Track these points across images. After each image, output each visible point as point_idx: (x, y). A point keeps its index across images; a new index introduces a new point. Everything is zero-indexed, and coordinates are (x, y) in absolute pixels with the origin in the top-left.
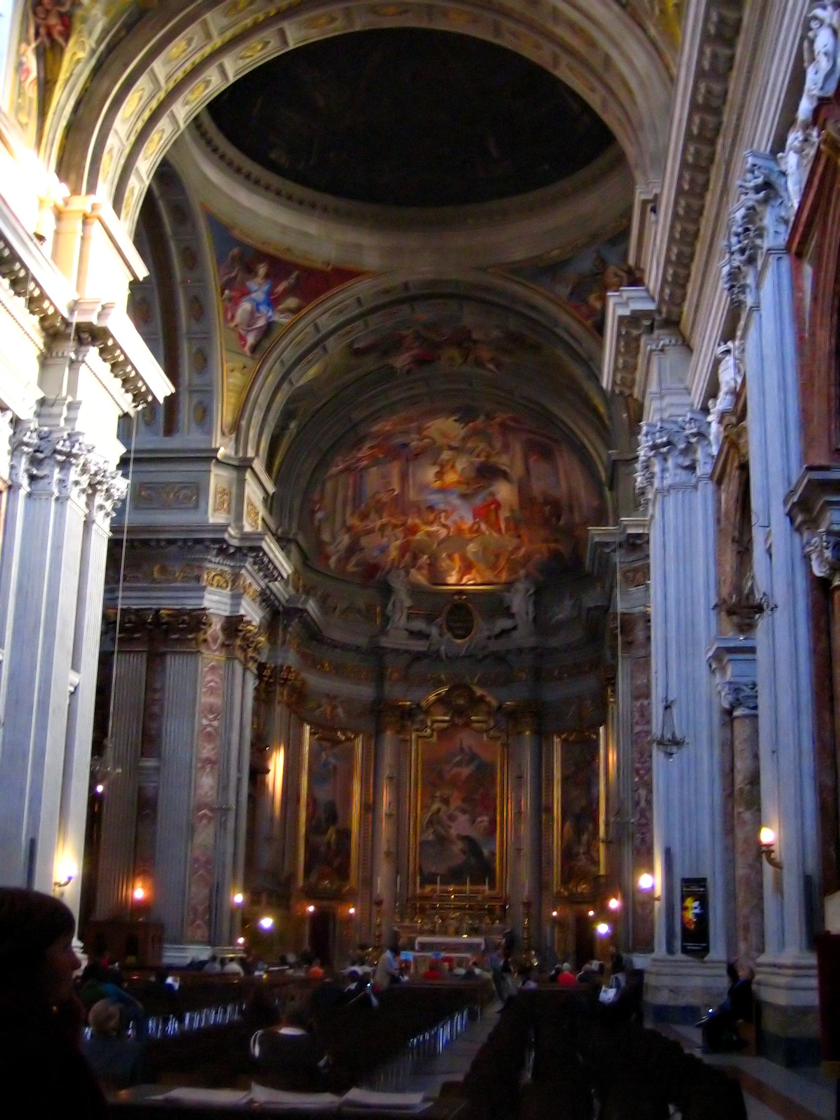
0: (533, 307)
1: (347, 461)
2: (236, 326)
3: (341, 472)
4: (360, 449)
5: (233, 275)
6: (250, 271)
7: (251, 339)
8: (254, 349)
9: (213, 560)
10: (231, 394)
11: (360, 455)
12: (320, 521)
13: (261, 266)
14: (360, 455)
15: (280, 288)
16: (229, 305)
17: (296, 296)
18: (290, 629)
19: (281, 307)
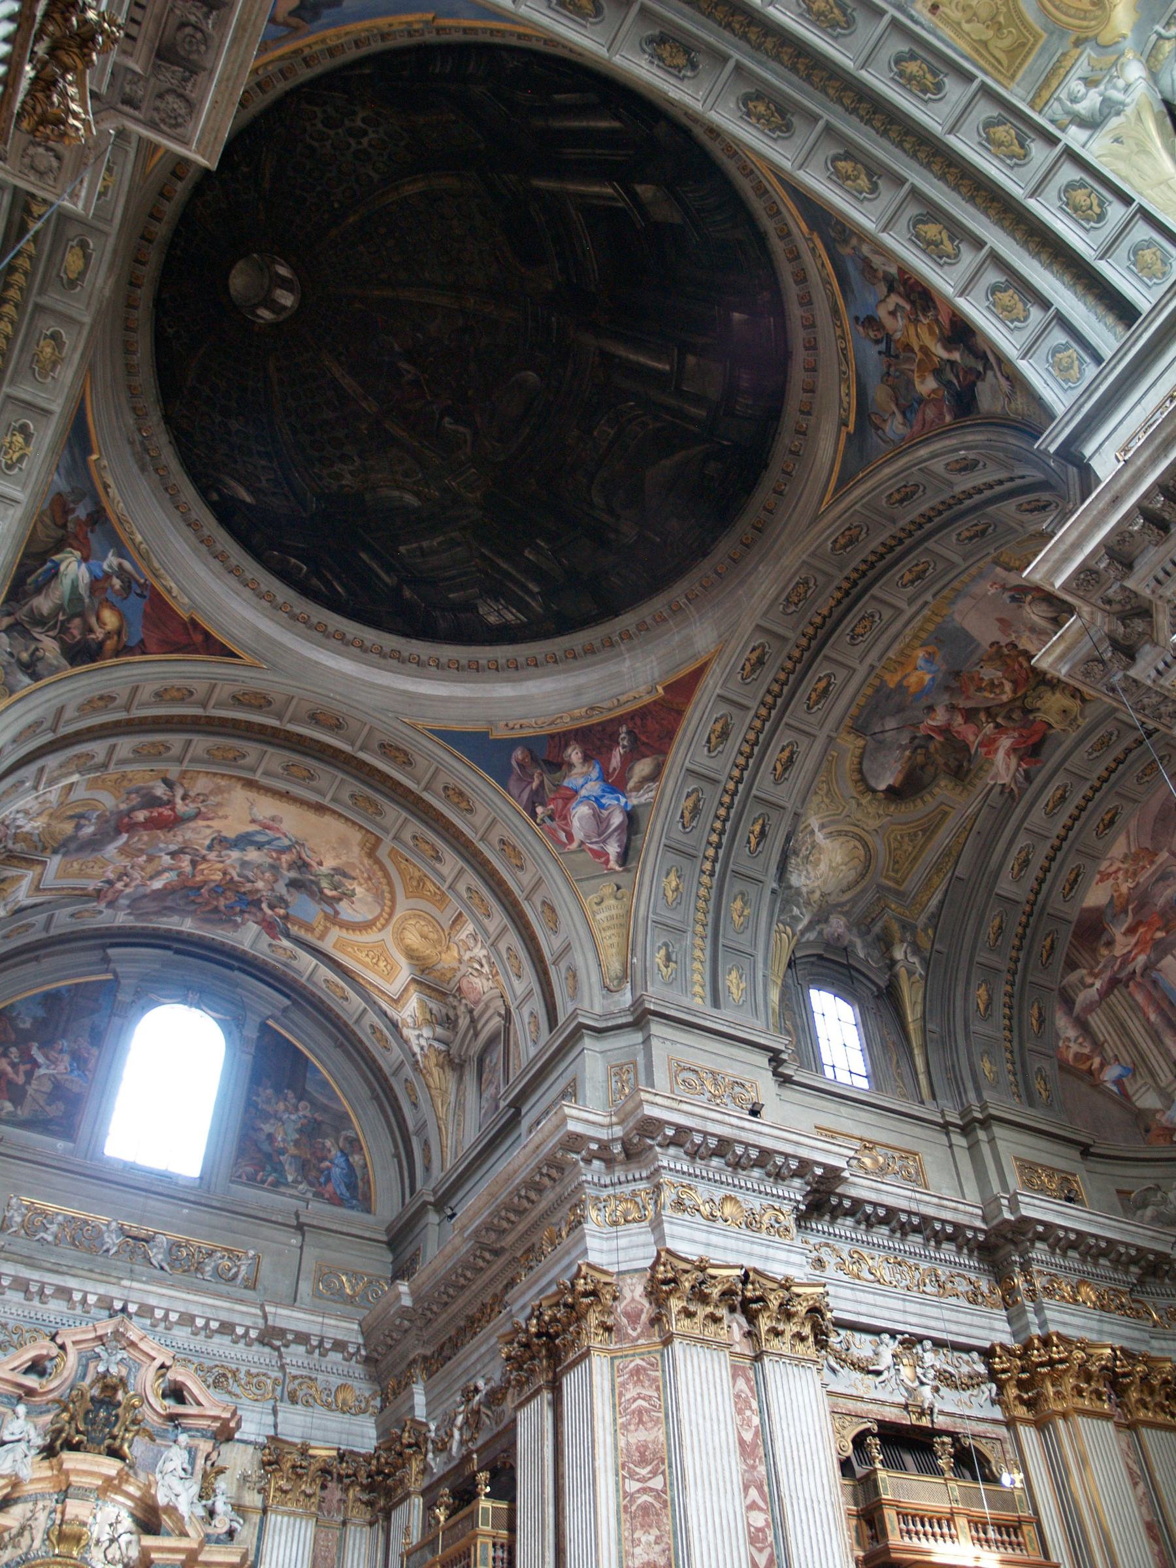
0: (907, 495)
1: (1101, 972)
2: (582, 843)
3: (1105, 994)
4: (1110, 943)
5: (535, 785)
6: (558, 765)
7: (613, 849)
8: (624, 857)
9: (608, 1182)
10: (608, 933)
11: (1119, 951)
12: (1118, 1082)
13: (569, 750)
14: (1119, 951)
15: (616, 761)
16: (554, 825)
17: (644, 756)
18: (1035, 1267)
19: (631, 784)
